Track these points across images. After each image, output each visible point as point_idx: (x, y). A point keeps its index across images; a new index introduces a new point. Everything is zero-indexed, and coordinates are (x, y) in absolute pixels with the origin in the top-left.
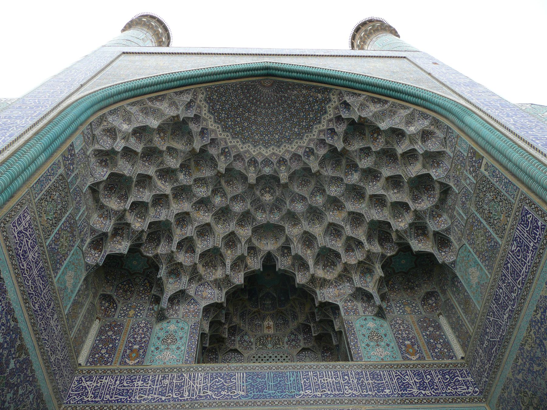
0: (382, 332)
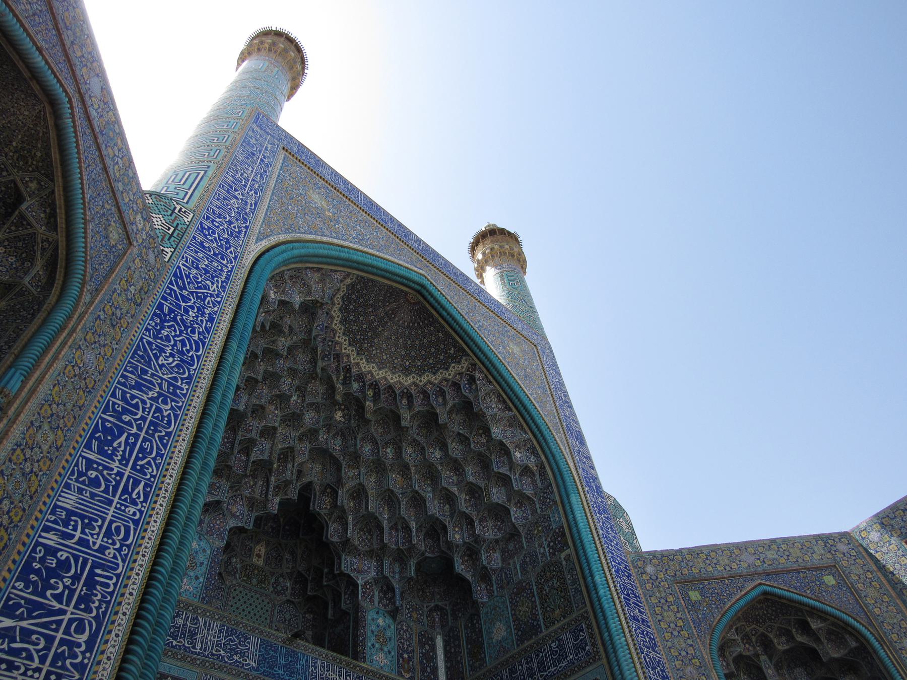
0: (389, 634)
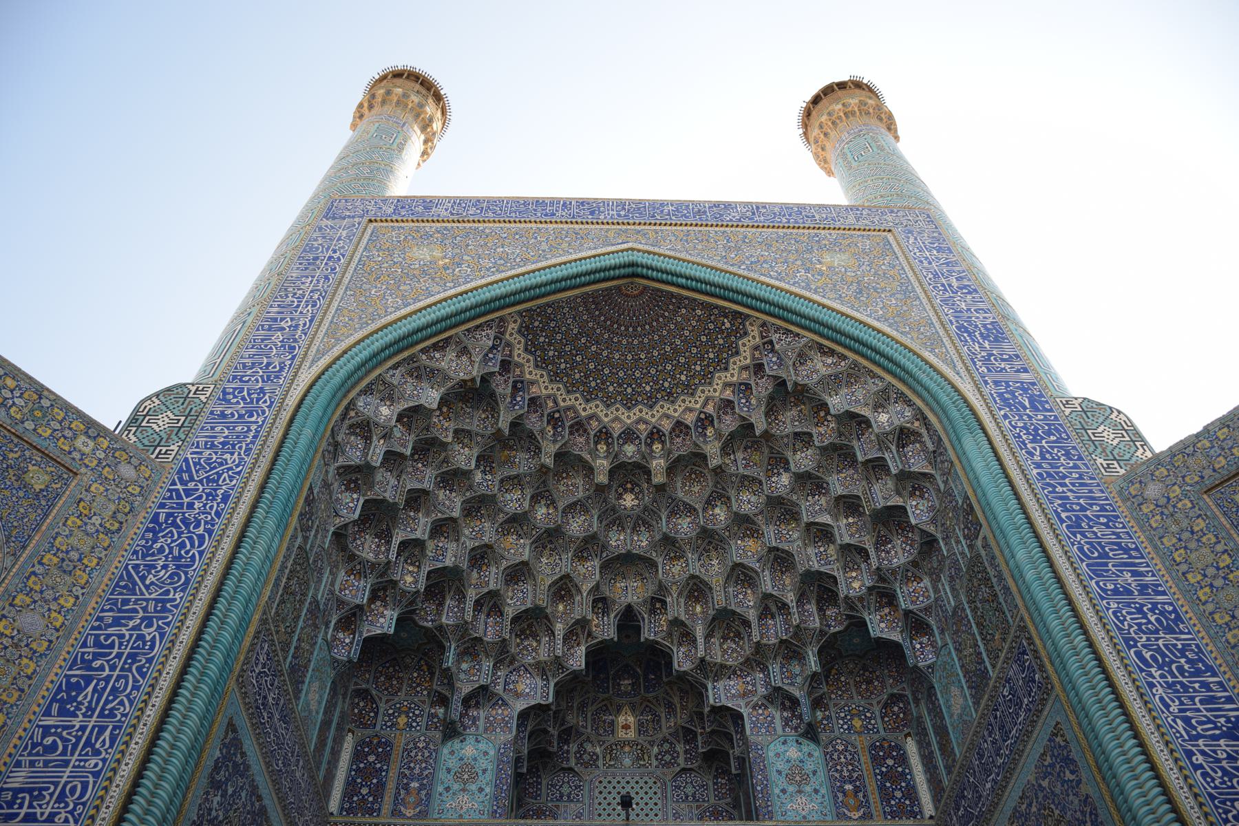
0: (809, 766)
